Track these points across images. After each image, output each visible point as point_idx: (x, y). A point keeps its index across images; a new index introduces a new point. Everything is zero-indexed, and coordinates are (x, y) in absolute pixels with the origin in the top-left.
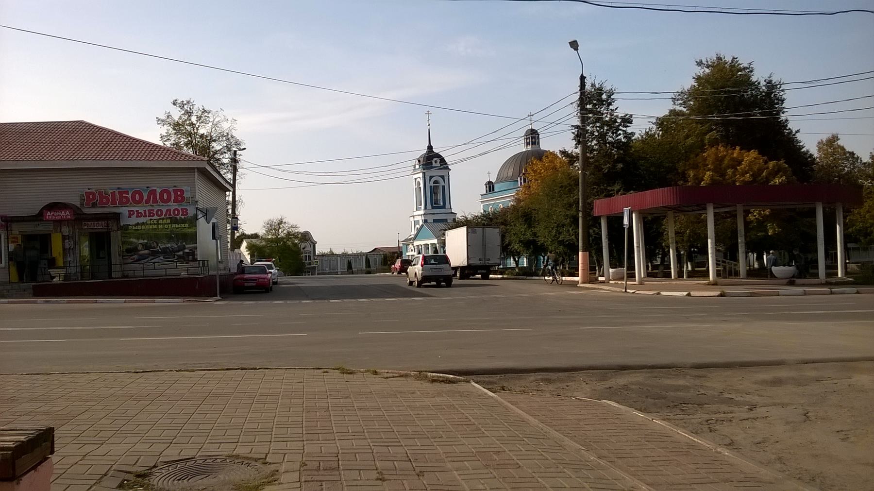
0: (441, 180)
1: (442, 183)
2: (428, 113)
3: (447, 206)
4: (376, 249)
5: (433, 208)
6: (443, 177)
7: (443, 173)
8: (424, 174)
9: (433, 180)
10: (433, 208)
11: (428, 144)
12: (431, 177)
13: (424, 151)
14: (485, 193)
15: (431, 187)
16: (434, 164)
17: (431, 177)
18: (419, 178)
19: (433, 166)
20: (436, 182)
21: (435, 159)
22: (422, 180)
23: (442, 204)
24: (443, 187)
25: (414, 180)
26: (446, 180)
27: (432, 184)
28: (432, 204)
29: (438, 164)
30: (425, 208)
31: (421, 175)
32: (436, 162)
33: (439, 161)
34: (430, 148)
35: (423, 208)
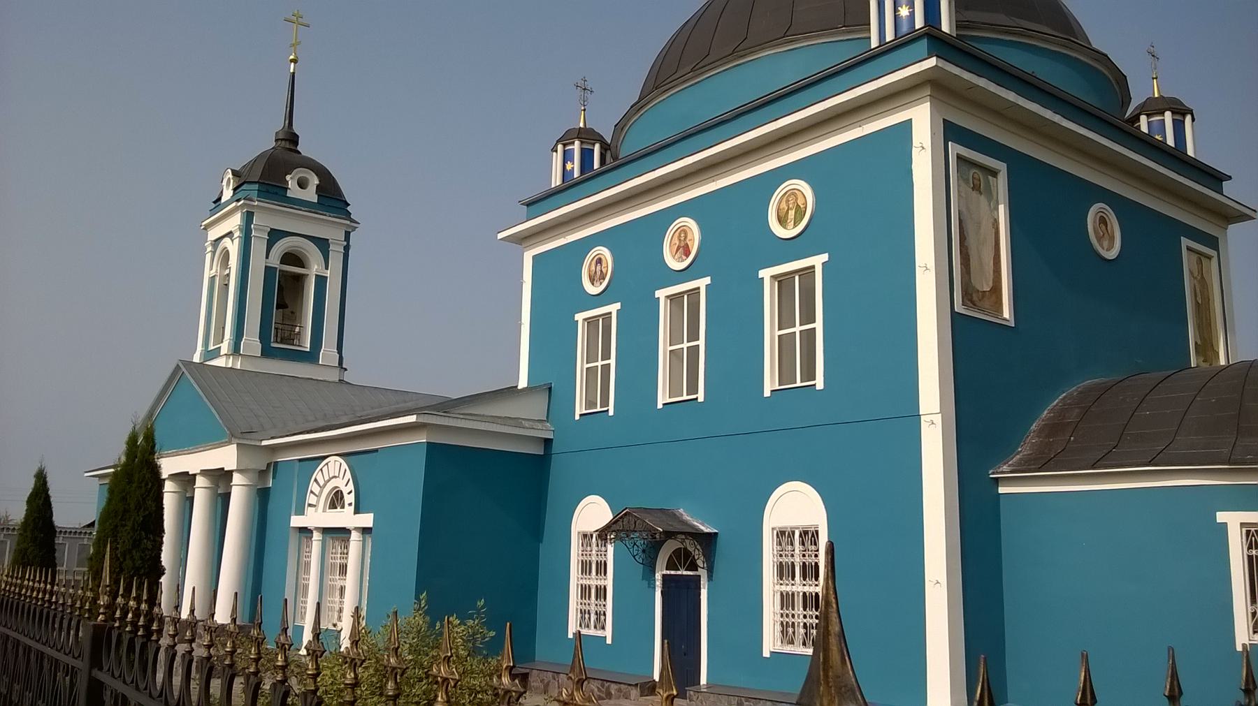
1: (315, 267)
2: (296, 20)
3: (328, 353)
5: (267, 352)
7: (330, 230)
8: (249, 217)
9: (282, 246)
10: (267, 352)
11: (279, 124)
14: (556, 181)
15: (269, 270)
16: (294, 191)
17: (275, 236)
19: (289, 194)
20: (292, 258)
21: (300, 173)
22: (237, 241)
23: (307, 345)
24: (321, 280)
25: (209, 249)
27: (275, 261)
28: (264, 337)
29: (310, 195)
30: (236, 350)
32: (302, 184)
33: (314, 181)
34: (291, 138)
35: (225, 347)
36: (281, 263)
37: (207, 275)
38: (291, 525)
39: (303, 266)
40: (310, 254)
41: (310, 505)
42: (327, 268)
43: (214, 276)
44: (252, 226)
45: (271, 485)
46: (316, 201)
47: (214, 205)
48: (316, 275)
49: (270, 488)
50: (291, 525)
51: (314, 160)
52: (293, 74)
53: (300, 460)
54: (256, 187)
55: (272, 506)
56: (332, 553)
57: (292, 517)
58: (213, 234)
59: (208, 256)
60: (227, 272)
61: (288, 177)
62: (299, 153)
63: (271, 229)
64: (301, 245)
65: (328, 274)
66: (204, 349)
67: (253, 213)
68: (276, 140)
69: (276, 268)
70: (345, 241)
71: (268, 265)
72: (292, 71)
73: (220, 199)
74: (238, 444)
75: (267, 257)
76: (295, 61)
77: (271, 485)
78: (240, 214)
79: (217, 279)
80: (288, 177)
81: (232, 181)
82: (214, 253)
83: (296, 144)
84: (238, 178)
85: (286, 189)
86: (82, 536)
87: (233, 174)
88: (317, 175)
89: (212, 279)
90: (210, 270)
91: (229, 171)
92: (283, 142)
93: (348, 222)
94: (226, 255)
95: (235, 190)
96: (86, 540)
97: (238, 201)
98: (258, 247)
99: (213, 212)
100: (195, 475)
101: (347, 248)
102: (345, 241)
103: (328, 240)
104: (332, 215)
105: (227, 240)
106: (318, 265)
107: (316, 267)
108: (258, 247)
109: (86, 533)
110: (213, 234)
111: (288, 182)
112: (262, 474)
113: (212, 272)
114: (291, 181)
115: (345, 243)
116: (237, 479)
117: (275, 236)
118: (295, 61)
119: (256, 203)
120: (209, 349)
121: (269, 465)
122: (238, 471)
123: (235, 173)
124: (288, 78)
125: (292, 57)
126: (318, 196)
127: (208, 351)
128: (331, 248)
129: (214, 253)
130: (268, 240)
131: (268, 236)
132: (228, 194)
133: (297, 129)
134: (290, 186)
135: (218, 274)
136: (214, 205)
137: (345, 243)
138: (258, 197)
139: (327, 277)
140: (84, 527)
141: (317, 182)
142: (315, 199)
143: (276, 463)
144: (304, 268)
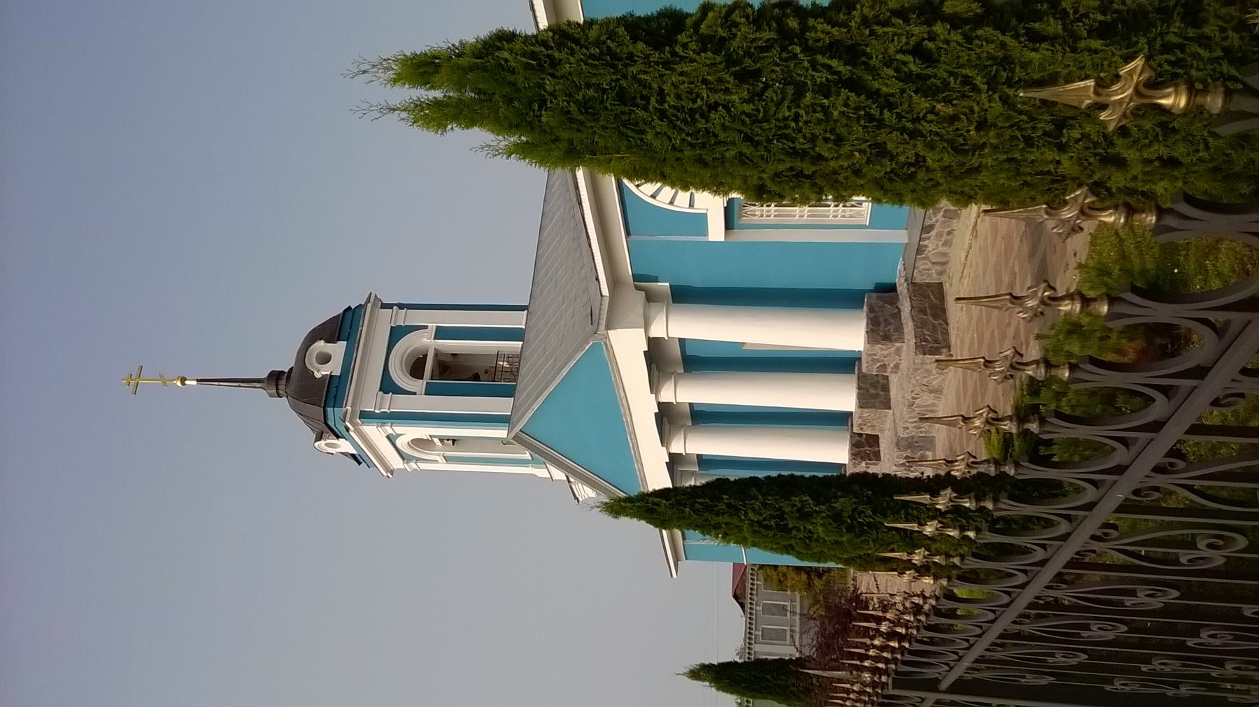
0: (408, 344)
1: (425, 341)
4: (736, 596)
6: (397, 333)
7: (379, 327)
8: (365, 416)
9: (400, 378)
11: (260, 395)
12: (388, 386)
13: (281, 408)
16: (333, 368)
18: (391, 439)
20: (416, 369)
22: (399, 429)
24: (441, 333)
25: (413, 465)
26: (415, 318)
27: (419, 385)
29: (338, 350)
31: (376, 433)
32: (325, 359)
33: (320, 346)
34: (276, 378)
36: (422, 379)
37: (443, 466)
38: (723, 240)
39: (425, 356)
40: (411, 346)
41: (691, 205)
42: (426, 327)
43: (444, 457)
44: (377, 411)
45: (668, 284)
46: (346, 342)
47: (363, 463)
48: (435, 338)
49: (670, 285)
50: (723, 240)
51: (298, 352)
52: (197, 380)
53: (628, 233)
54: (330, 410)
55: (696, 280)
56: (762, 216)
57: (710, 240)
58: (396, 462)
59: (423, 466)
60: (436, 440)
61: (318, 375)
62: (292, 368)
63: (380, 390)
64: (399, 356)
65: (432, 326)
66: (530, 465)
67: (361, 411)
68: (279, 396)
69: (427, 383)
70: (392, 308)
71: (423, 393)
72: (195, 383)
73: (353, 456)
74: (608, 327)
75: (415, 394)
76: (183, 380)
77: (668, 284)
78: (364, 427)
79: (447, 454)
80: (318, 375)
81: (328, 441)
82: (418, 460)
83: (282, 373)
84: (325, 434)
85: (331, 377)
86: (754, 612)
87: (320, 440)
88: (313, 343)
89: (447, 459)
90: (436, 462)
91: (317, 444)
92: (280, 387)
93: (369, 305)
94: (418, 443)
95: (338, 437)
96: (758, 608)
97: (347, 429)
98: (401, 404)
99: (370, 465)
100: (659, 404)
101: (401, 306)
102: (392, 308)
103: (392, 327)
104: (361, 324)
105: (398, 442)
106: (423, 336)
107: (425, 339)
108: (401, 404)
109: (751, 608)
110: (396, 462)
111: (323, 376)
112: (651, 298)
113: (440, 461)
114: (321, 372)
115: (395, 307)
116: (657, 331)
117: (388, 386)
118: (183, 380)
119: (349, 408)
120: (530, 458)
121: (638, 288)
122: (647, 327)
123: (319, 438)
124: (206, 387)
125: (179, 384)
126: (339, 340)
127: (533, 459)
128: (402, 324)
129: (418, 460)
130: (393, 393)
131: (389, 393)
132: (345, 446)
133: (264, 375)
134: (328, 373)
135: (442, 452)
136: (363, 463)
137: (395, 307)
138: (342, 407)
139: (437, 327)
140: (744, 611)
141: (322, 343)
142: (342, 345)
143: (636, 278)
144: (427, 355)
